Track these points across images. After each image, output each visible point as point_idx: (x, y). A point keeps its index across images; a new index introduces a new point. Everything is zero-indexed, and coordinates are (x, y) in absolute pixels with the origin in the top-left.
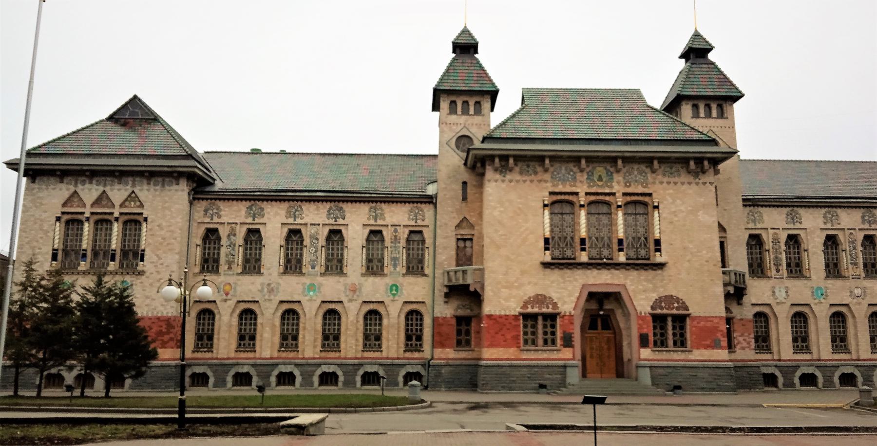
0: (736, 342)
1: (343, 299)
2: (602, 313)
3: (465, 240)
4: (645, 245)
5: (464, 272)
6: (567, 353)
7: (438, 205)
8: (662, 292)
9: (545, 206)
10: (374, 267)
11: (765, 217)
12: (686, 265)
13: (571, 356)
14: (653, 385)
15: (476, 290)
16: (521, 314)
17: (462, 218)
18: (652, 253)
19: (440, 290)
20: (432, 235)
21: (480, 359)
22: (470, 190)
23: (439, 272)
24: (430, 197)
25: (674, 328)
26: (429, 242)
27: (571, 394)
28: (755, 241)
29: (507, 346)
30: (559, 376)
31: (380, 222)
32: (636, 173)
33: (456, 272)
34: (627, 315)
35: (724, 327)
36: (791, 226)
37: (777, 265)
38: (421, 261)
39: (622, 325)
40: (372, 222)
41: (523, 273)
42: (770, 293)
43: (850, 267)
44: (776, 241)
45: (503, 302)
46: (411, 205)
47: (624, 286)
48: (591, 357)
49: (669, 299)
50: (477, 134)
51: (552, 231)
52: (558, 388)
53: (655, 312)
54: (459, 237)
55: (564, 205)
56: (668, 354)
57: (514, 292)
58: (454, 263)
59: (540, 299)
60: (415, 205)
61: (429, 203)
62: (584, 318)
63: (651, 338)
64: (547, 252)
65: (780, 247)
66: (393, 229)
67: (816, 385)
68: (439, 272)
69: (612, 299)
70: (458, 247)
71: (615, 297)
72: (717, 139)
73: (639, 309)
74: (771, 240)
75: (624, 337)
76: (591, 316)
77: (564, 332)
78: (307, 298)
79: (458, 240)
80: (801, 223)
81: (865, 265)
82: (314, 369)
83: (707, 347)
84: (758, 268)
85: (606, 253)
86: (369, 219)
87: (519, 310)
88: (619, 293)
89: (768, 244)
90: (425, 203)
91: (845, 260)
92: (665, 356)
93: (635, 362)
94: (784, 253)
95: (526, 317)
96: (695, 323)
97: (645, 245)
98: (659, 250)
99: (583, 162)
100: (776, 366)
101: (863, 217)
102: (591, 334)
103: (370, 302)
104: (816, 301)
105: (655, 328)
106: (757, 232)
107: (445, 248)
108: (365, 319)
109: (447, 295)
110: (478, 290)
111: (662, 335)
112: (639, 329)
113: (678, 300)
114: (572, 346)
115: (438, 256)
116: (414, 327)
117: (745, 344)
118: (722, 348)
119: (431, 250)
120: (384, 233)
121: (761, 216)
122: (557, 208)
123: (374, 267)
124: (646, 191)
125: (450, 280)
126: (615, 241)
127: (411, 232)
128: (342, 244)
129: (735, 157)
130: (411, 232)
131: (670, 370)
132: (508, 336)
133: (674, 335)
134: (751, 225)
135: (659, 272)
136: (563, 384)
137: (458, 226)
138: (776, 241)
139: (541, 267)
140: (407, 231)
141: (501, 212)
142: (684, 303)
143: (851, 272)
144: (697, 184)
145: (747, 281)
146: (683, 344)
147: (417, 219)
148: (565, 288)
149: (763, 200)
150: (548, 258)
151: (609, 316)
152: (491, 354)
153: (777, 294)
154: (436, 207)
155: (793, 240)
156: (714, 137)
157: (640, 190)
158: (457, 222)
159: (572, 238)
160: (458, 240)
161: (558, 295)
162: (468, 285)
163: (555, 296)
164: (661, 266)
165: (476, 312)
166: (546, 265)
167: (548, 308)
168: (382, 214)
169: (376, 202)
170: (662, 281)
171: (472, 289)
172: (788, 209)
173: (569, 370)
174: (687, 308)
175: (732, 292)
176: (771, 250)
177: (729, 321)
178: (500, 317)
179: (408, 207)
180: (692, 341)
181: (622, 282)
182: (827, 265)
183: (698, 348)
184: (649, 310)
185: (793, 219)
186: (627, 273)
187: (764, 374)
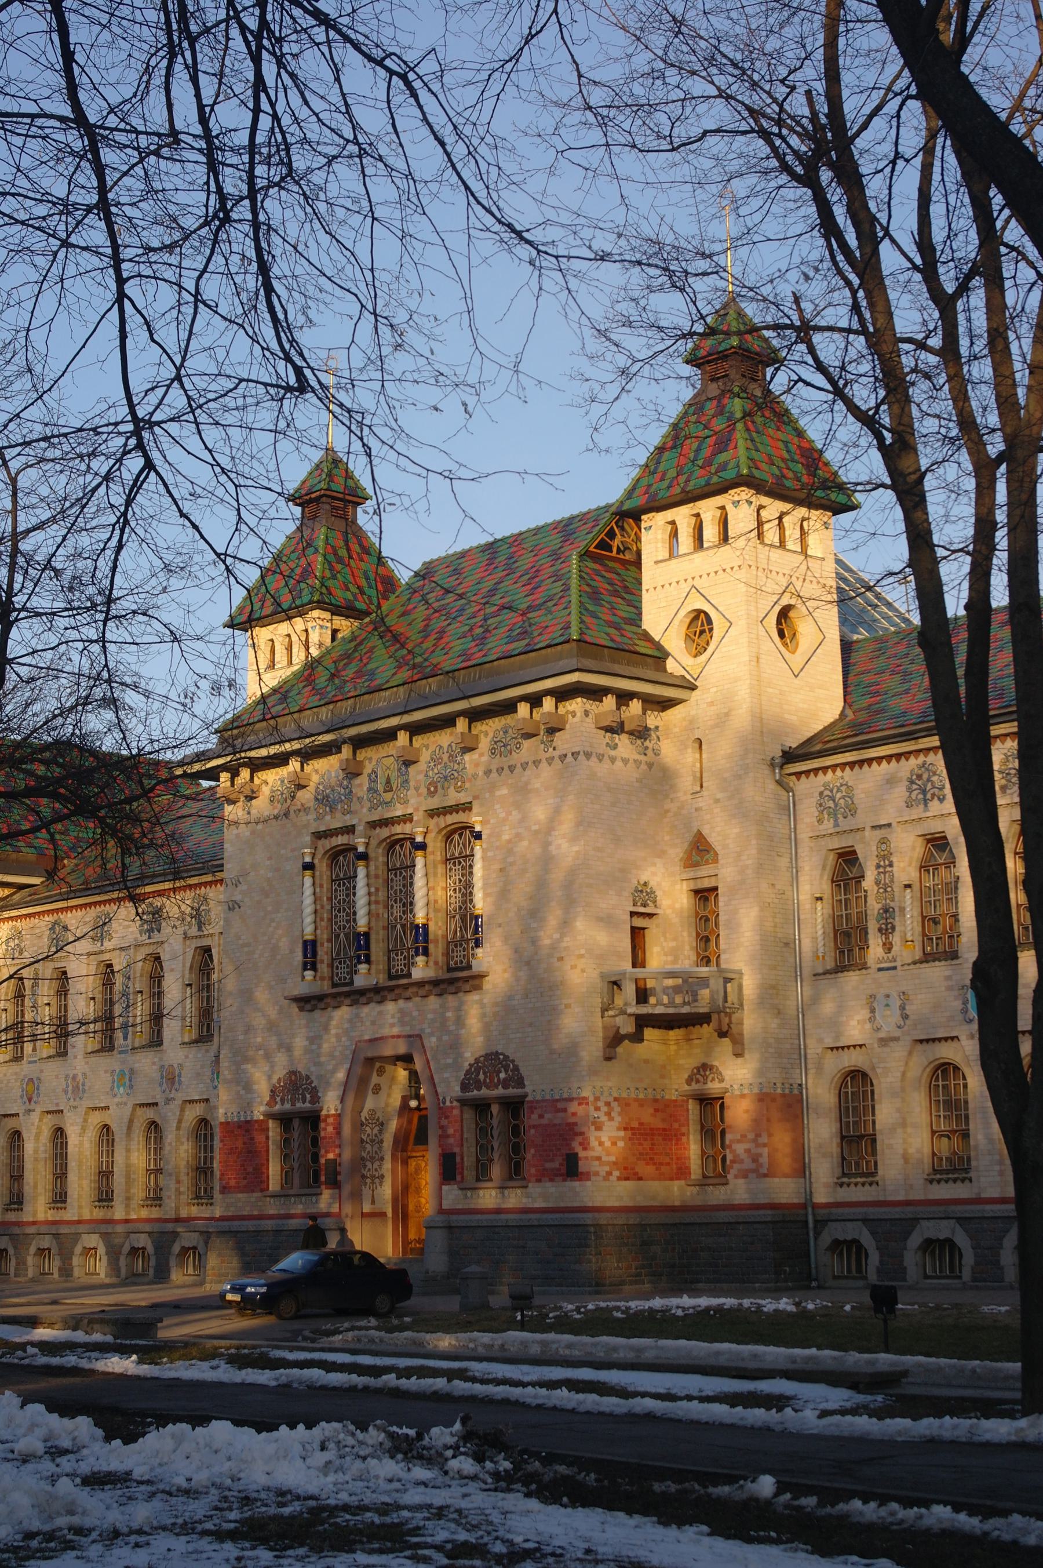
1: (159, 1098)
9: (309, 867)
32: (445, 757)
47: (419, 1036)
78: (116, 1100)
83: (552, 1176)
96: (535, 1116)
100: (865, 1221)
124: (463, 798)
139: (294, 1009)
142: (516, 1069)
144: (550, 761)
157: (454, 797)
166: (307, 1003)
172: (913, 762)
183: (539, 1181)
185: (924, 792)
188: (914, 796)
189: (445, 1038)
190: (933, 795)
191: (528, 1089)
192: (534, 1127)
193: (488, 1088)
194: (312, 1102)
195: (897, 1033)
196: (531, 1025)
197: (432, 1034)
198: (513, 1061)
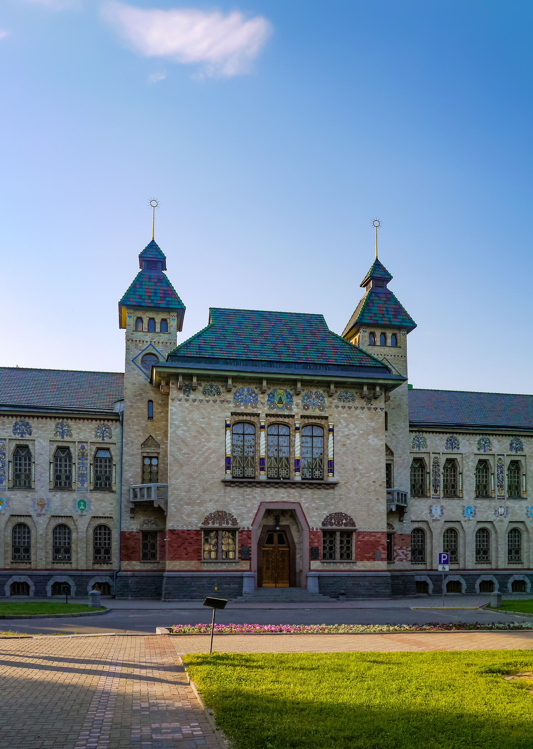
0: (395, 554)
1: (32, 513)
2: (278, 528)
3: (151, 458)
4: (320, 466)
5: (149, 489)
6: (245, 565)
7: (124, 423)
8: (333, 510)
10: (62, 483)
11: (428, 442)
12: (356, 485)
13: (248, 568)
14: (320, 593)
15: (159, 506)
16: (202, 529)
17: (147, 435)
18: (325, 474)
19: (126, 507)
20: (118, 452)
21: (164, 571)
22: (157, 409)
23: (125, 488)
24: (117, 414)
25: (342, 542)
26: (116, 459)
27: (246, 602)
28: (419, 464)
29: (189, 558)
30: (236, 586)
31: (66, 438)
33: (141, 489)
34: (300, 530)
35: (384, 541)
36: (450, 451)
37: (436, 486)
38: (109, 479)
39: (296, 540)
40: (59, 438)
41: (205, 490)
42: (428, 511)
43: (497, 488)
44: (436, 464)
45: (184, 517)
46: (98, 422)
48: (267, 568)
49: (339, 517)
50: (164, 352)
51: (233, 451)
52: (235, 596)
53: (325, 527)
54: (145, 455)
55: (246, 426)
56: (335, 565)
57: (196, 508)
58: (140, 480)
59: (221, 515)
60: (102, 422)
61: (116, 420)
62: (262, 532)
63: (321, 551)
64: (229, 472)
65: (439, 470)
66: (80, 446)
67: (460, 592)
68: (125, 488)
69: (287, 516)
70: (144, 465)
71: (291, 514)
72: (390, 366)
73: (311, 524)
74: (432, 464)
75: (297, 551)
76: (269, 531)
77: (242, 546)
79: (144, 457)
80: (458, 449)
81: (510, 487)
82: (5, 579)
83: (369, 559)
84: (419, 490)
85: (283, 473)
86: (55, 435)
87: (200, 525)
88: (294, 510)
89: (430, 468)
90: (112, 420)
91: (493, 482)
92: (332, 567)
93: (305, 572)
94: (442, 476)
95: (208, 531)
96: (360, 538)
97: (320, 466)
98: (332, 471)
99: (265, 383)
101: (511, 445)
102: (268, 548)
103: (59, 517)
104: (466, 519)
105: (324, 542)
106: (421, 456)
107: (131, 465)
108: (54, 532)
109: (132, 511)
110: (162, 506)
111: (331, 548)
112: (310, 542)
113: (346, 517)
114: (250, 559)
115: (124, 473)
116: (103, 541)
117: (403, 557)
118: (382, 560)
119: (118, 467)
120: (72, 450)
121: (425, 440)
122: (239, 429)
123: (62, 483)
125: (135, 496)
126: (292, 461)
127: (99, 449)
128: (30, 460)
129: (404, 384)
130: (99, 449)
131: (335, 579)
132: (190, 550)
133: (341, 548)
134: (416, 450)
135: (331, 491)
136: (239, 593)
137: (144, 444)
138: (436, 464)
140: (94, 448)
141: (185, 431)
142: (351, 519)
143: (497, 493)
145: (408, 501)
146: (349, 556)
147: (103, 437)
148: (245, 506)
149: (427, 426)
150: (229, 477)
151: (284, 531)
152: (173, 566)
153: (433, 512)
154: (122, 425)
155: (452, 465)
156: (387, 364)
158: (142, 440)
159: (253, 458)
160: (144, 457)
161: (238, 512)
162: (153, 502)
163: (234, 512)
164: (333, 485)
165: (161, 527)
166: (226, 483)
167: (228, 524)
168: (69, 431)
169: (63, 418)
170: (333, 499)
171: (156, 505)
173: (245, 580)
174: (353, 524)
175: (394, 509)
176: (431, 472)
177: (389, 536)
178: (183, 532)
179: (94, 424)
180: (356, 554)
181: (298, 500)
182: (478, 487)
184: (321, 525)
186: (302, 492)
187: (417, 582)
188: (448, 445)
189: (314, 505)
190: (455, 447)
191: (357, 527)
192: (360, 541)
193: (336, 525)
194: (233, 524)
195: (439, 518)
196: (359, 504)
197: (305, 503)
198: (350, 517)
